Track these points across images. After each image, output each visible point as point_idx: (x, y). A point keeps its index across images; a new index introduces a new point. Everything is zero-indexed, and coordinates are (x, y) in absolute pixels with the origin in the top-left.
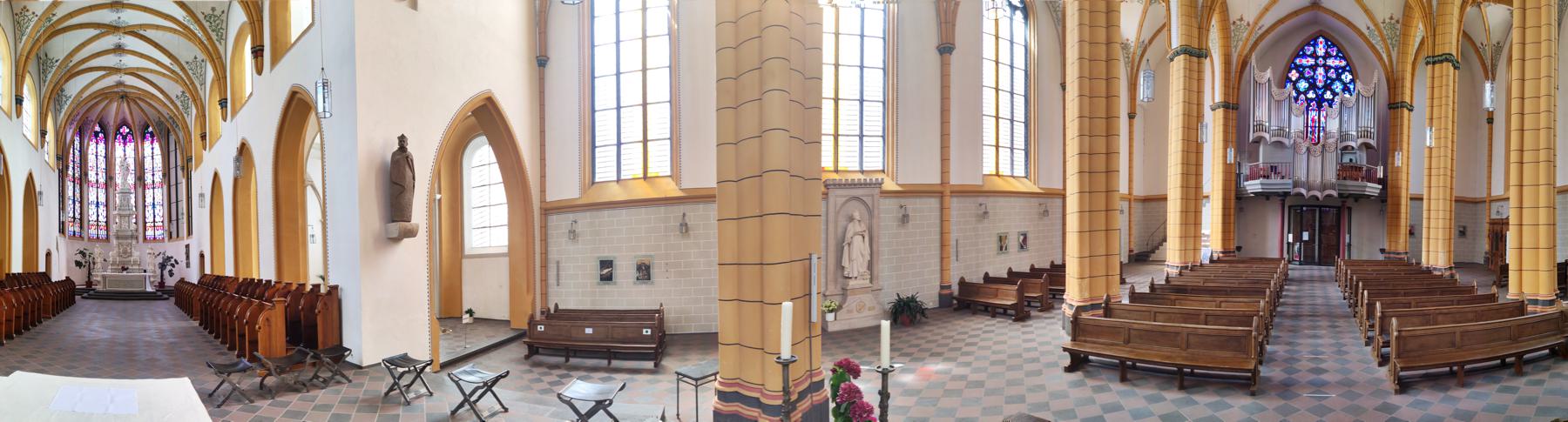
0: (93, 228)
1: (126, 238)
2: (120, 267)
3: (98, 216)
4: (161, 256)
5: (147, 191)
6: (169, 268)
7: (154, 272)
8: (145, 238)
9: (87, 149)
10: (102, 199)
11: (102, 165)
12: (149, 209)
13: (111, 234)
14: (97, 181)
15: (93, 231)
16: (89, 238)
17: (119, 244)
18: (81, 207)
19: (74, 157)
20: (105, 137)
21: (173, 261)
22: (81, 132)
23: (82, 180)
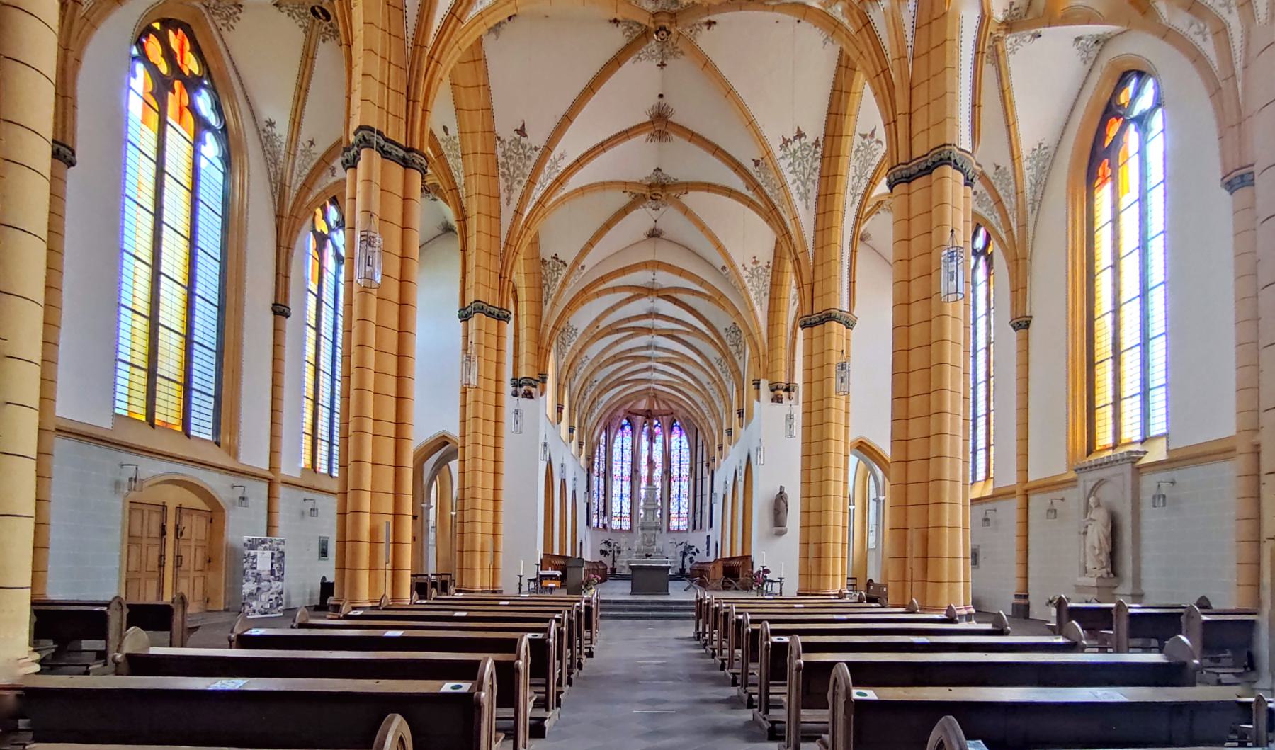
0: (617, 519)
1: (650, 529)
2: (644, 554)
3: (622, 507)
4: (683, 545)
5: (673, 483)
6: (690, 555)
7: (675, 558)
8: (669, 529)
9: (613, 442)
10: (627, 490)
11: (628, 458)
12: (674, 501)
13: (636, 525)
14: (622, 474)
15: (616, 524)
16: (612, 530)
17: (644, 535)
18: (605, 500)
19: (599, 453)
20: (632, 430)
21: (694, 550)
22: (607, 429)
23: (608, 474)
